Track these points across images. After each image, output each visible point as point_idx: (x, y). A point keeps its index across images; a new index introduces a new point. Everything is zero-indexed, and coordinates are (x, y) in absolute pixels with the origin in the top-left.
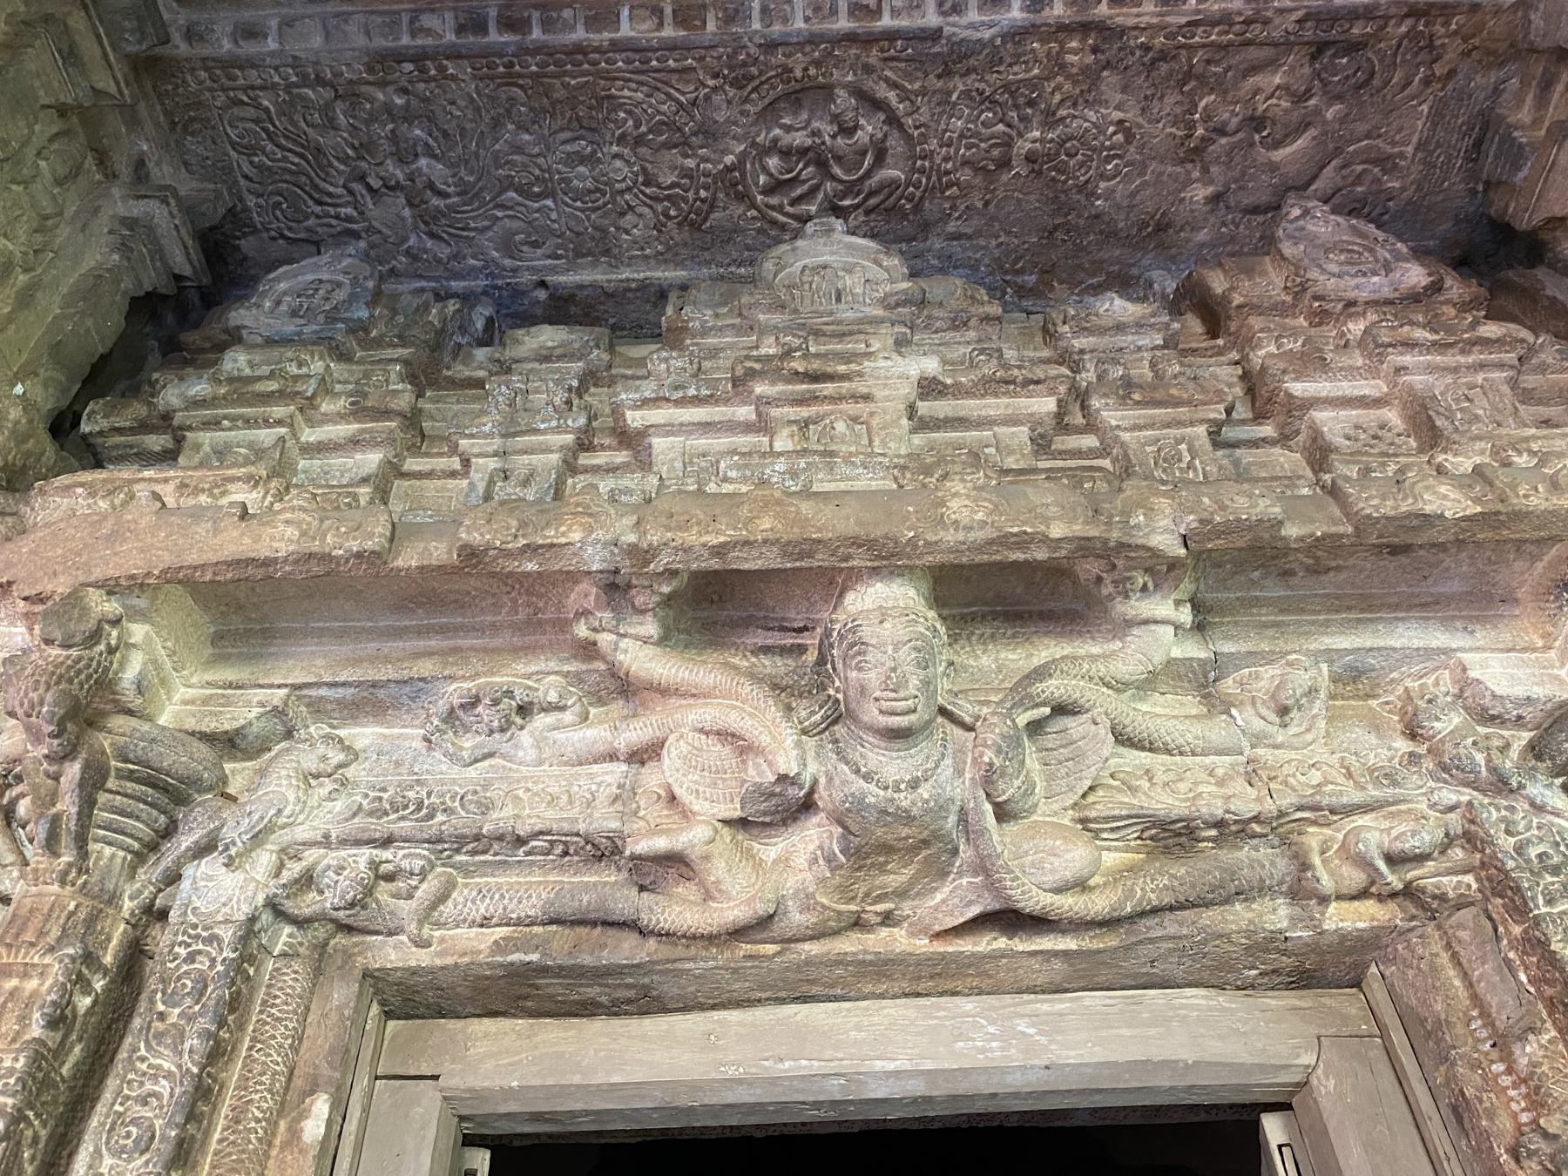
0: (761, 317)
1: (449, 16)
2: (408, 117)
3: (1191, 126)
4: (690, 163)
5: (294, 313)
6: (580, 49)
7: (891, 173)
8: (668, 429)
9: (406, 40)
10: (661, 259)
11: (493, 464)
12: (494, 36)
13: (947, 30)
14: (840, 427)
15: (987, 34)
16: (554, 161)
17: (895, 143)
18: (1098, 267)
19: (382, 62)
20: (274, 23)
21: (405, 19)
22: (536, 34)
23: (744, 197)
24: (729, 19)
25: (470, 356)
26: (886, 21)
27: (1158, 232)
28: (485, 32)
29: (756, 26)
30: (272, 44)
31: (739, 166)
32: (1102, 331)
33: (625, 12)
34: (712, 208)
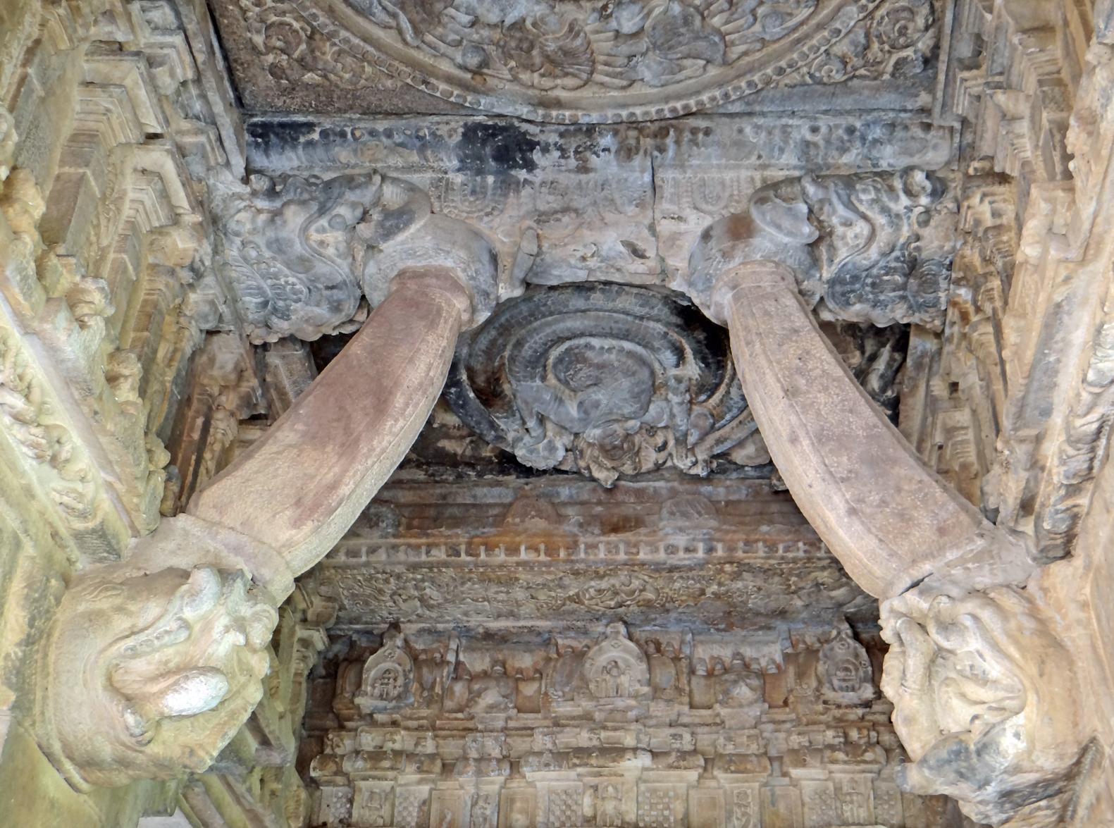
0: (584, 704)
1: (443, 548)
2: (423, 580)
3: (789, 586)
4: (553, 594)
5: (381, 697)
6: (501, 566)
7: (650, 595)
8: (543, 780)
9: (424, 558)
10: (538, 618)
11: (472, 790)
12: (464, 557)
13: (669, 562)
14: (610, 789)
15: (687, 562)
16: (491, 594)
17: (648, 587)
18: (755, 624)
19: (414, 567)
20: (364, 550)
21: (424, 549)
22: (483, 556)
23: (580, 602)
24: (569, 555)
25: (452, 693)
26: (643, 556)
27: (782, 614)
28: (458, 555)
29: (582, 555)
30: (364, 559)
31: (577, 595)
32: (733, 707)
33: (523, 548)
34: (564, 605)
